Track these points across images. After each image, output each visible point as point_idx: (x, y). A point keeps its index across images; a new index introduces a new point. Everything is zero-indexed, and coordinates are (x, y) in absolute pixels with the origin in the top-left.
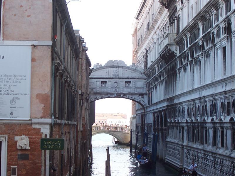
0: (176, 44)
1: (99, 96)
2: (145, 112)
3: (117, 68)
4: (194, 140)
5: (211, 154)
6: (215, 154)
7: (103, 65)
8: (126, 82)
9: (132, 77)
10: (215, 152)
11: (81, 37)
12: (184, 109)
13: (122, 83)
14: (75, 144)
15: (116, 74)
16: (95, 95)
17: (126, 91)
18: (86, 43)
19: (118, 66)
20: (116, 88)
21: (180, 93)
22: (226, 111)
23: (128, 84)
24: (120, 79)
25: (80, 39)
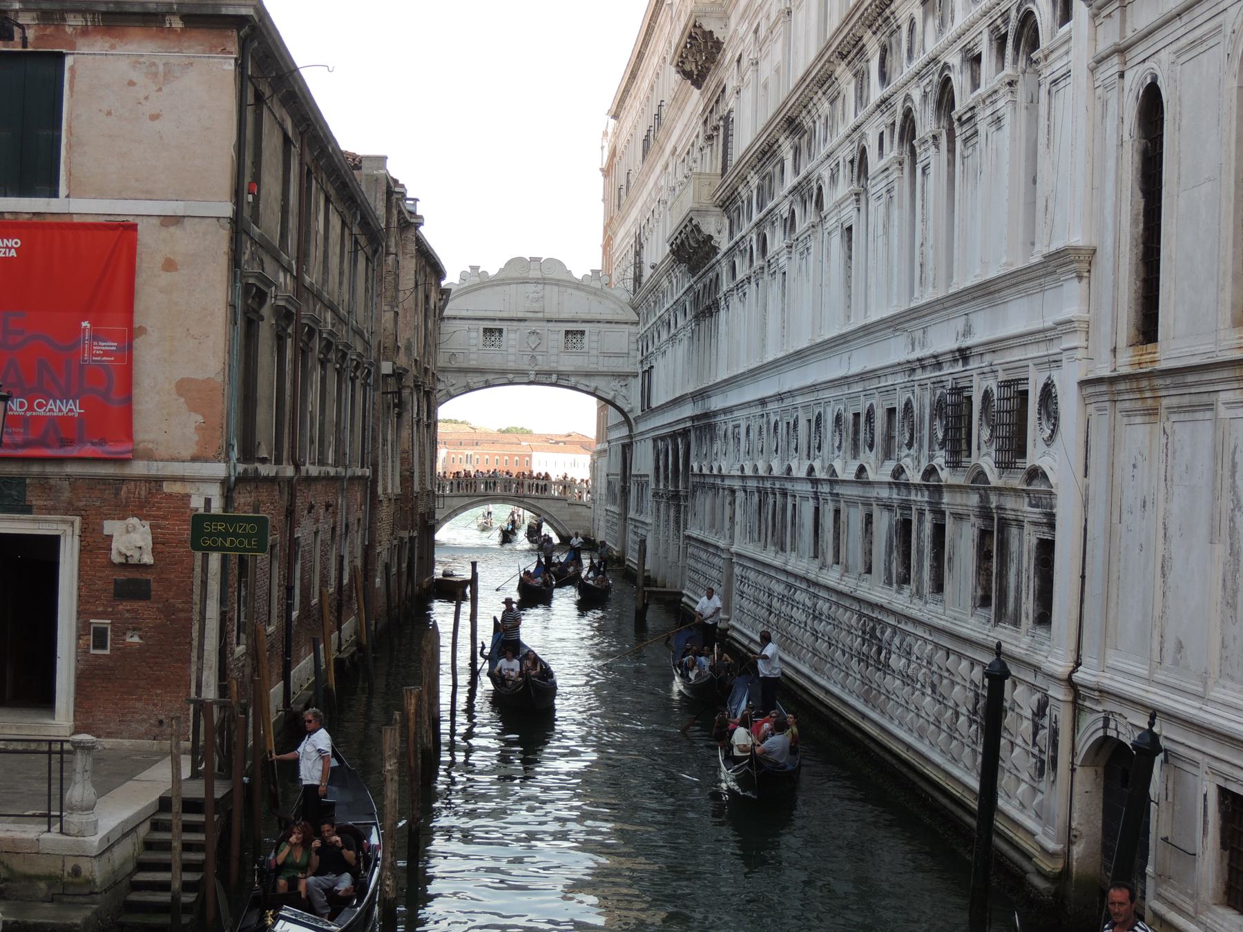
2: (630, 437)
3: (540, 287)
4: (763, 536)
5: (804, 586)
6: (816, 584)
10: (815, 580)
11: (396, 181)
12: (737, 430)
13: (555, 337)
15: (536, 306)
16: (463, 374)
17: (568, 363)
18: (416, 200)
21: (725, 377)
22: (847, 444)
23: (574, 341)
24: (549, 321)
25: (389, 187)
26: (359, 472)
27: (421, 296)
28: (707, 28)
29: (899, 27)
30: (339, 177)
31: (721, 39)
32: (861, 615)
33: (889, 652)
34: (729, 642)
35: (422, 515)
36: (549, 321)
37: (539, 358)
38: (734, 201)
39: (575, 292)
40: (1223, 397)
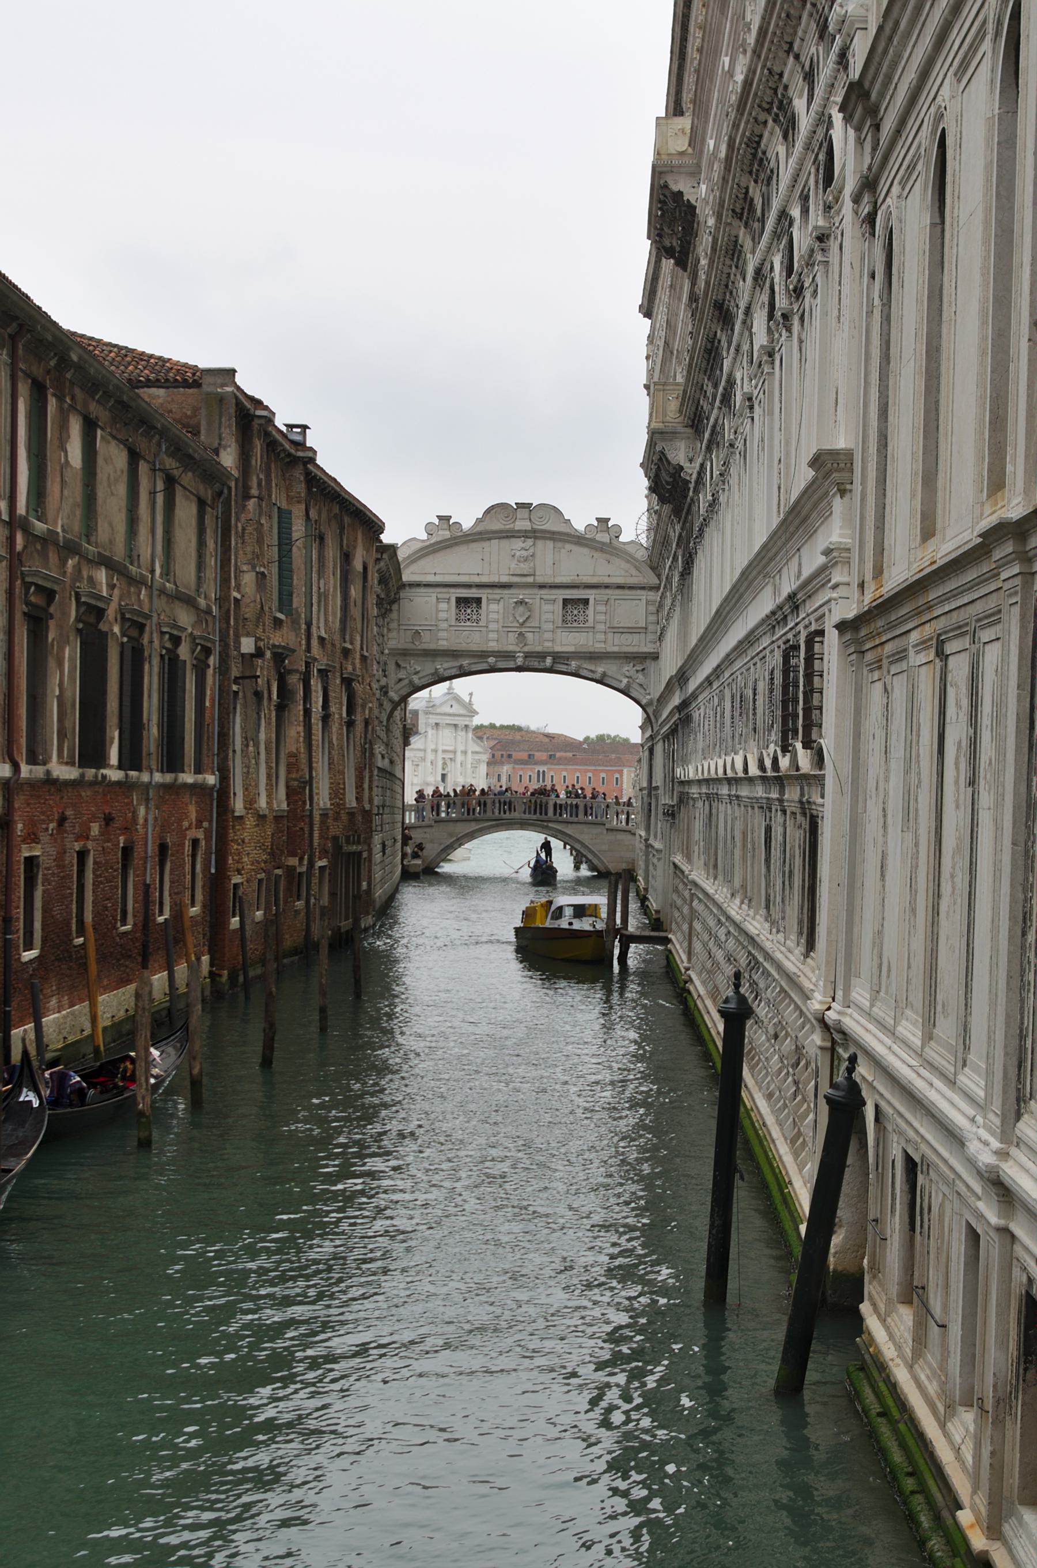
0: (689, 430)
1: (446, 665)
3: (530, 542)
7: (467, 523)
8: (566, 602)
9: (594, 580)
11: (258, 403)
14: (213, 871)
15: (524, 568)
16: (429, 659)
17: (567, 642)
18: (305, 427)
19: (534, 531)
20: (523, 630)
23: (576, 612)
24: (542, 586)
26: (188, 778)
27: (332, 553)
28: (675, 188)
29: (772, 171)
30: (107, 395)
31: (693, 202)
32: (750, 953)
33: (760, 1000)
34: (686, 998)
35: (335, 839)
36: (542, 586)
37: (530, 636)
38: (700, 421)
39: (577, 549)
40: (914, 637)
